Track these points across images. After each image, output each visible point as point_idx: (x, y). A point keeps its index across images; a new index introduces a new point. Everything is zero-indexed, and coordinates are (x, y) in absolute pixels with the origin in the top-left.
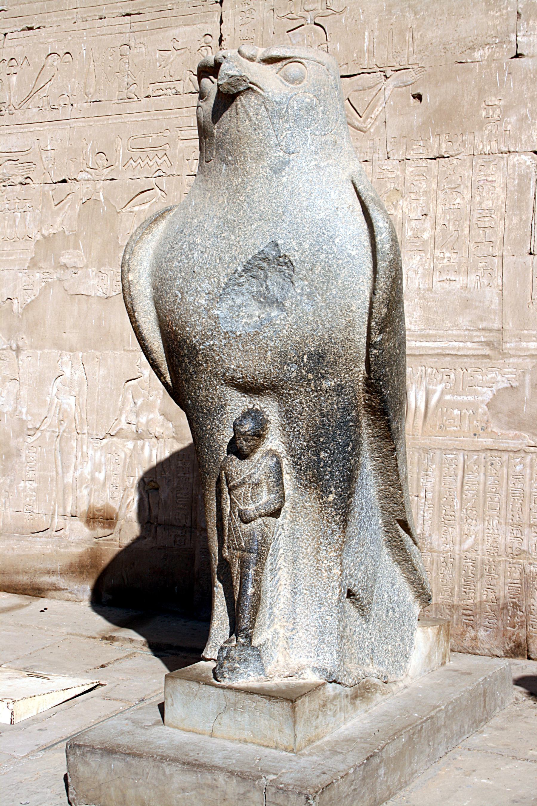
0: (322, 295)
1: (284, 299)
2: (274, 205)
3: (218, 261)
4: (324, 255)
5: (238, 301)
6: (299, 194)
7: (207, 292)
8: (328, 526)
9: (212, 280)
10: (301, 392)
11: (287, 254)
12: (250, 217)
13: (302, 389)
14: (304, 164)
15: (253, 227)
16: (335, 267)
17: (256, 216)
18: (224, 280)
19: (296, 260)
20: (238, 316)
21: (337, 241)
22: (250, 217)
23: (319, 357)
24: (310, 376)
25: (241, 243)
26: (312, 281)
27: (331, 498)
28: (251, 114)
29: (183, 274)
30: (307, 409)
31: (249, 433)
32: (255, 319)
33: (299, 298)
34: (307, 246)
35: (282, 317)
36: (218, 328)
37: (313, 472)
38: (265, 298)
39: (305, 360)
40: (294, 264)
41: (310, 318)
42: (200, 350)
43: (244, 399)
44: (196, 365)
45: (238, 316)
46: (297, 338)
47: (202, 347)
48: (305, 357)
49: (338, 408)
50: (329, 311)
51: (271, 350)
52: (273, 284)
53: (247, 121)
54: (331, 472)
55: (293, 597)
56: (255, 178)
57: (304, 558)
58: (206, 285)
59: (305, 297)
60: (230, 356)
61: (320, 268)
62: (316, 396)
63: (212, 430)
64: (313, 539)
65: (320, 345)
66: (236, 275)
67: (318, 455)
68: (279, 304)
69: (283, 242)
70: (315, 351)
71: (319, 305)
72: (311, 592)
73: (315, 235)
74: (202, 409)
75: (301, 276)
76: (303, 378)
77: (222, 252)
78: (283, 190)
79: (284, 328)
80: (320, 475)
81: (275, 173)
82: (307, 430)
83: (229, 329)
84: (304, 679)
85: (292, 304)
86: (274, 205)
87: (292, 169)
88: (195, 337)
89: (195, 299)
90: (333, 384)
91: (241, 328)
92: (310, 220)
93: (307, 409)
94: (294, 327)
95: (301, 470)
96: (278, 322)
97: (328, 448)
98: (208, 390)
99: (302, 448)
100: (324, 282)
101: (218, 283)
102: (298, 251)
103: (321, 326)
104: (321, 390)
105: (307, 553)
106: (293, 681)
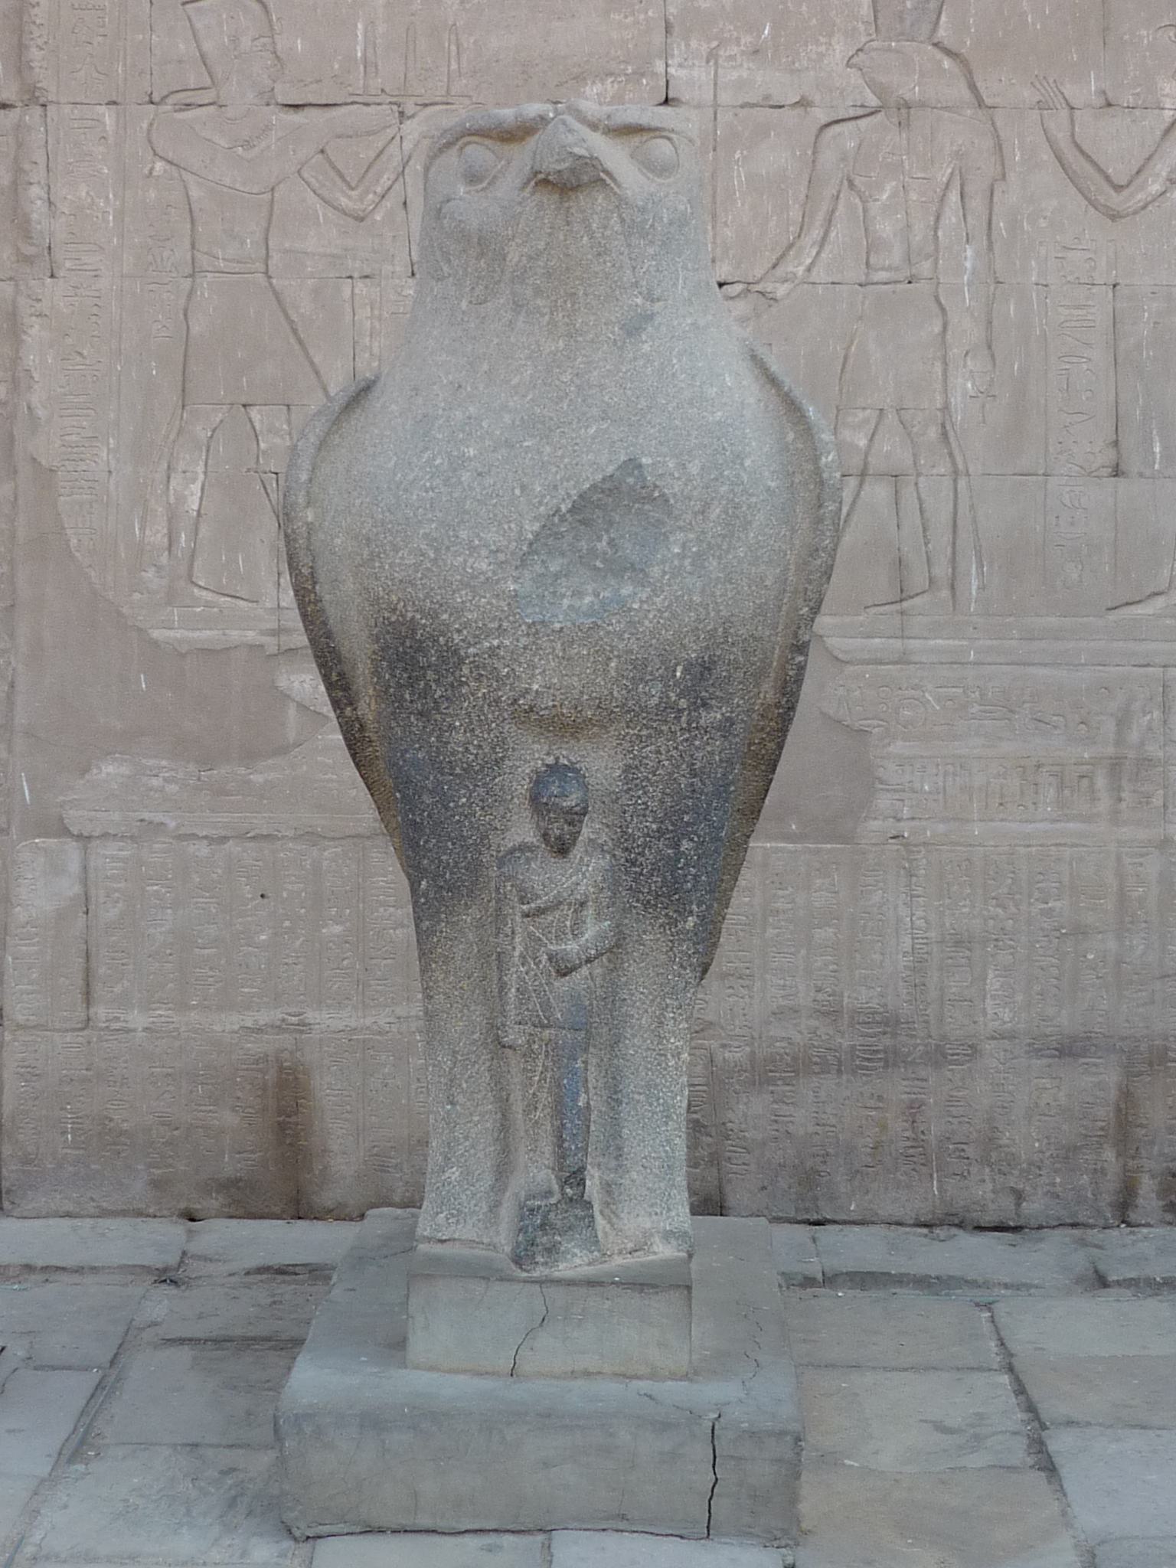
0: (720, 558)
2: (629, 393)
3: (517, 492)
6: (673, 375)
7: (493, 548)
10: (662, 731)
13: (664, 728)
15: (592, 431)
17: (595, 411)
18: (531, 528)
19: (675, 495)
20: (554, 593)
21: (747, 463)
22: (584, 414)
23: (703, 669)
27: (691, 921)
29: (439, 515)
30: (666, 763)
31: (577, 809)
32: (587, 600)
33: (676, 563)
34: (694, 469)
35: (644, 596)
37: (665, 877)
38: (605, 561)
40: (672, 501)
41: (696, 599)
43: (536, 746)
44: (452, 685)
46: (669, 635)
47: (471, 650)
48: (679, 669)
49: (721, 760)
51: (619, 657)
52: (622, 537)
54: (695, 876)
55: (613, 1108)
56: (592, 341)
57: (634, 1036)
58: (492, 536)
59: (687, 562)
60: (534, 667)
62: (687, 740)
63: (470, 807)
64: (653, 1001)
65: (707, 648)
66: (556, 519)
67: (677, 846)
68: (637, 571)
69: (650, 461)
70: (697, 658)
74: (451, 768)
75: (681, 523)
76: (673, 707)
77: (525, 474)
79: (646, 617)
81: (630, 334)
83: (538, 618)
84: (655, 1253)
85: (665, 573)
86: (629, 393)
88: (459, 631)
89: (465, 561)
90: (719, 716)
91: (561, 617)
93: (666, 763)
94: (666, 614)
95: (641, 874)
96: (636, 606)
98: (473, 730)
99: (648, 835)
100: (724, 537)
101: (520, 532)
102: (679, 479)
103: (712, 614)
106: (641, 1258)
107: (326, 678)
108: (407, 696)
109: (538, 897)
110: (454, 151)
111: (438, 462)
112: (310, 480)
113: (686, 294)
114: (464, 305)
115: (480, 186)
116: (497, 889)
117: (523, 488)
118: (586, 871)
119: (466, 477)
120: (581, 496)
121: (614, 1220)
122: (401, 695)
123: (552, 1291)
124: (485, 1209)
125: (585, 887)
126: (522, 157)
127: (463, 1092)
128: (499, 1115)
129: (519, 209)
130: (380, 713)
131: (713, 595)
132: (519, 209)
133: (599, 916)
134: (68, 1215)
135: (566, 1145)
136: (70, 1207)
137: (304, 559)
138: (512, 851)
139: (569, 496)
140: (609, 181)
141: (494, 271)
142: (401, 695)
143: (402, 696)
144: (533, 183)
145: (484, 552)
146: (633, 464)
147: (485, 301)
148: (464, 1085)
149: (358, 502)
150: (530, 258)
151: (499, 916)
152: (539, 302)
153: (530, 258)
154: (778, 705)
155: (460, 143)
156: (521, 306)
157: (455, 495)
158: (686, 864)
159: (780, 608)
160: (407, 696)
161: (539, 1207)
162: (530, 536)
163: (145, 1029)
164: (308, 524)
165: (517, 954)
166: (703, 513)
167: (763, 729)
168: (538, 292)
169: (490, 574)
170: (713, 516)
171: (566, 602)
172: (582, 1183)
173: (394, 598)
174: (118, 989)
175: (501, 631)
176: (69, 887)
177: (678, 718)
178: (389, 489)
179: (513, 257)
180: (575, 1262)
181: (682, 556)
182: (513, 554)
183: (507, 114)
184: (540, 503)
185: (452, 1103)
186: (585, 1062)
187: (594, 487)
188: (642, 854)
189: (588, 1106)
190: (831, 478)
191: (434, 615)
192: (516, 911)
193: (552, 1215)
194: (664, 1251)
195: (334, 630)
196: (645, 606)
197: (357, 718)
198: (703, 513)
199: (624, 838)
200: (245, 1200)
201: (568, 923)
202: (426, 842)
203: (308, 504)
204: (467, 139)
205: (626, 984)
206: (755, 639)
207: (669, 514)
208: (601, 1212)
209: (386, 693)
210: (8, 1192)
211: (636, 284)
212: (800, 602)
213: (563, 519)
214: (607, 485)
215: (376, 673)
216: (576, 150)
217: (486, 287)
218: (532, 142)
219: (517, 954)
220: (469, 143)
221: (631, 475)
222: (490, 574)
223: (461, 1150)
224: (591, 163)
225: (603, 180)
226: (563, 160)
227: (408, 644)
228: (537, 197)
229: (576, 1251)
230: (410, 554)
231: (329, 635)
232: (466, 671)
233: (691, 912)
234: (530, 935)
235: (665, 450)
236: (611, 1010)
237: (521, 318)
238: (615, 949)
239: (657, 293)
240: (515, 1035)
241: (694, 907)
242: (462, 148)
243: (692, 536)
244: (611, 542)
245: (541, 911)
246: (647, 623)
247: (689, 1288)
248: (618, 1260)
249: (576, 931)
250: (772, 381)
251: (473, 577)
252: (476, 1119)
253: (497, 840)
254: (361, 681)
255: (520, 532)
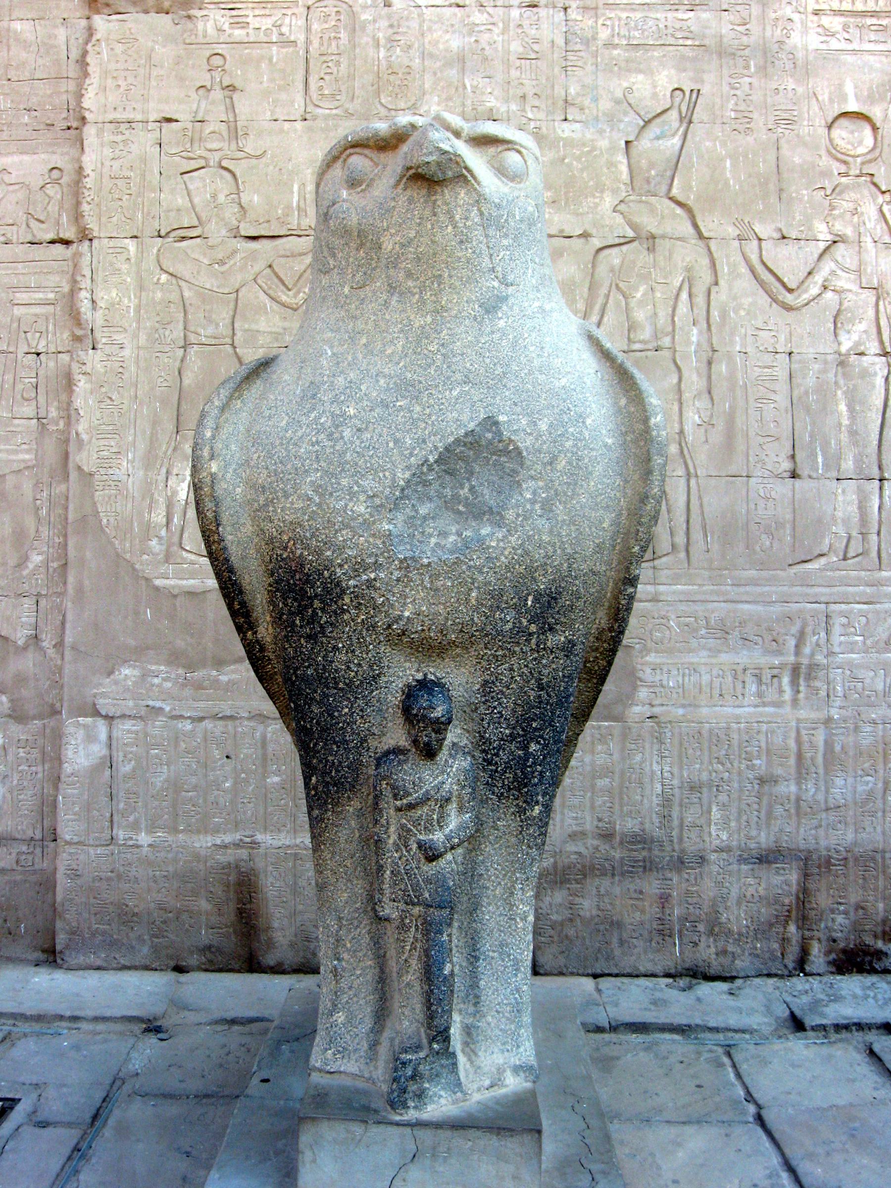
1: (504, 507)
2: (488, 361)
3: (391, 445)
4: (570, 443)
5: (423, 510)
7: (370, 493)
8: (527, 854)
9: (381, 475)
10: (515, 652)
11: (513, 438)
12: (448, 378)
13: (517, 649)
14: (526, 304)
15: (455, 393)
16: (586, 461)
17: (459, 376)
18: (403, 476)
19: (527, 448)
20: (423, 533)
21: (589, 421)
22: (448, 378)
24: (533, 628)
25: (433, 418)
26: (552, 481)
27: (537, 810)
28: (457, 217)
29: (323, 464)
30: (518, 679)
31: (443, 719)
32: (452, 538)
33: (528, 506)
34: (543, 426)
35: (500, 536)
36: (389, 552)
38: (466, 505)
39: (530, 603)
40: (525, 454)
42: (348, 588)
43: (408, 665)
44: (335, 612)
45: (423, 533)
46: (522, 569)
47: (352, 583)
48: (530, 598)
49: (564, 676)
50: (573, 528)
51: (478, 588)
53: (450, 228)
54: (541, 772)
55: (471, 963)
56: (456, 317)
57: (489, 904)
59: (537, 506)
60: (406, 597)
61: (564, 462)
62: (535, 659)
64: (505, 875)
65: (554, 580)
66: (425, 469)
67: (526, 748)
68: (495, 516)
69: (506, 419)
71: (559, 519)
72: (501, 954)
73: (556, 411)
74: (337, 683)
75: (533, 473)
78: (501, 339)
79: (502, 554)
80: (526, 777)
81: (488, 312)
82: (514, 711)
83: (409, 554)
85: (518, 515)
86: (488, 361)
87: (511, 308)
88: (341, 566)
89: (346, 505)
90: (563, 639)
91: (429, 554)
92: (547, 387)
93: (518, 679)
94: (519, 552)
95: (496, 771)
96: (493, 544)
97: (542, 737)
98: (353, 651)
99: (502, 739)
100: (568, 484)
102: (531, 434)
103: (559, 551)
104: (544, 649)
105: (494, 896)
107: (230, 606)
108: (298, 622)
109: (410, 794)
110: (339, 164)
111: (322, 421)
112: (213, 437)
113: (534, 281)
114: (346, 290)
115: (359, 189)
116: (375, 787)
117: (396, 441)
118: (450, 772)
119: (347, 433)
120: (446, 449)
121: (474, 1058)
122: (292, 619)
123: (420, 1133)
124: (366, 1046)
125: (450, 785)
126: (394, 163)
127: (348, 950)
128: (378, 970)
129: (393, 204)
130: (275, 637)
131: (559, 535)
132: (393, 204)
133: (461, 809)
134: (99, 968)
135: (434, 1008)
136: (99, 963)
137: (209, 505)
138: (387, 753)
139: (436, 448)
140: (470, 178)
141: (372, 259)
142: (292, 619)
143: (294, 621)
144: (405, 180)
145: (362, 498)
146: (491, 422)
147: (364, 286)
148: (349, 945)
149: (256, 455)
150: (403, 246)
151: (376, 806)
152: (410, 283)
153: (403, 246)
154: (611, 630)
155: (344, 156)
156: (395, 288)
157: (337, 448)
158: (534, 763)
159: (614, 547)
160: (298, 622)
161: (411, 1061)
162: (402, 483)
163: (150, 845)
164: (211, 475)
165: (391, 841)
166: (551, 464)
167: (597, 649)
168: (409, 275)
169: (367, 516)
170: (559, 467)
171: (433, 540)
172: (447, 1039)
173: (285, 538)
174: (131, 819)
175: (377, 566)
176: (98, 750)
177: (528, 641)
178: (282, 444)
179: (388, 245)
180: (440, 1104)
181: (533, 502)
182: (387, 498)
183: (382, 127)
184: (411, 455)
185: (338, 959)
186: (450, 935)
187: (457, 441)
188: (497, 755)
189: (452, 974)
190: (658, 436)
191: (319, 553)
192: (389, 806)
193: (421, 1067)
194: (513, 1083)
195: (236, 566)
196: (501, 544)
197: (257, 641)
198: (551, 464)
199: (482, 743)
200: (216, 963)
201: (435, 817)
202: (315, 745)
203: (212, 457)
204: (348, 152)
205: (483, 862)
206: (594, 573)
207: (522, 465)
208: (463, 1051)
209: (280, 619)
210: (61, 952)
211: (493, 270)
212: (632, 542)
213: (430, 469)
214: (470, 439)
215: (271, 602)
216: (441, 145)
217: (365, 274)
218: (405, 148)
219: (391, 841)
220: (351, 154)
221: (489, 431)
222: (367, 516)
223: (345, 998)
224: (454, 159)
225: (463, 175)
226: (431, 153)
227: (297, 577)
228: (409, 192)
229: (442, 1093)
230: (299, 497)
231: (231, 570)
232: (347, 600)
233: (537, 803)
234: (403, 826)
235: (519, 409)
236: (470, 883)
237: (395, 298)
238: (472, 840)
239: (511, 278)
240: (389, 910)
241: (540, 798)
242: (345, 160)
243: (541, 484)
244: (472, 488)
245: (411, 807)
246: (503, 559)
247: (539, 1132)
248: (477, 1097)
249: (441, 822)
250: (606, 355)
251: (353, 519)
252: (358, 972)
253: (376, 743)
254: (260, 609)
255: (393, 480)
